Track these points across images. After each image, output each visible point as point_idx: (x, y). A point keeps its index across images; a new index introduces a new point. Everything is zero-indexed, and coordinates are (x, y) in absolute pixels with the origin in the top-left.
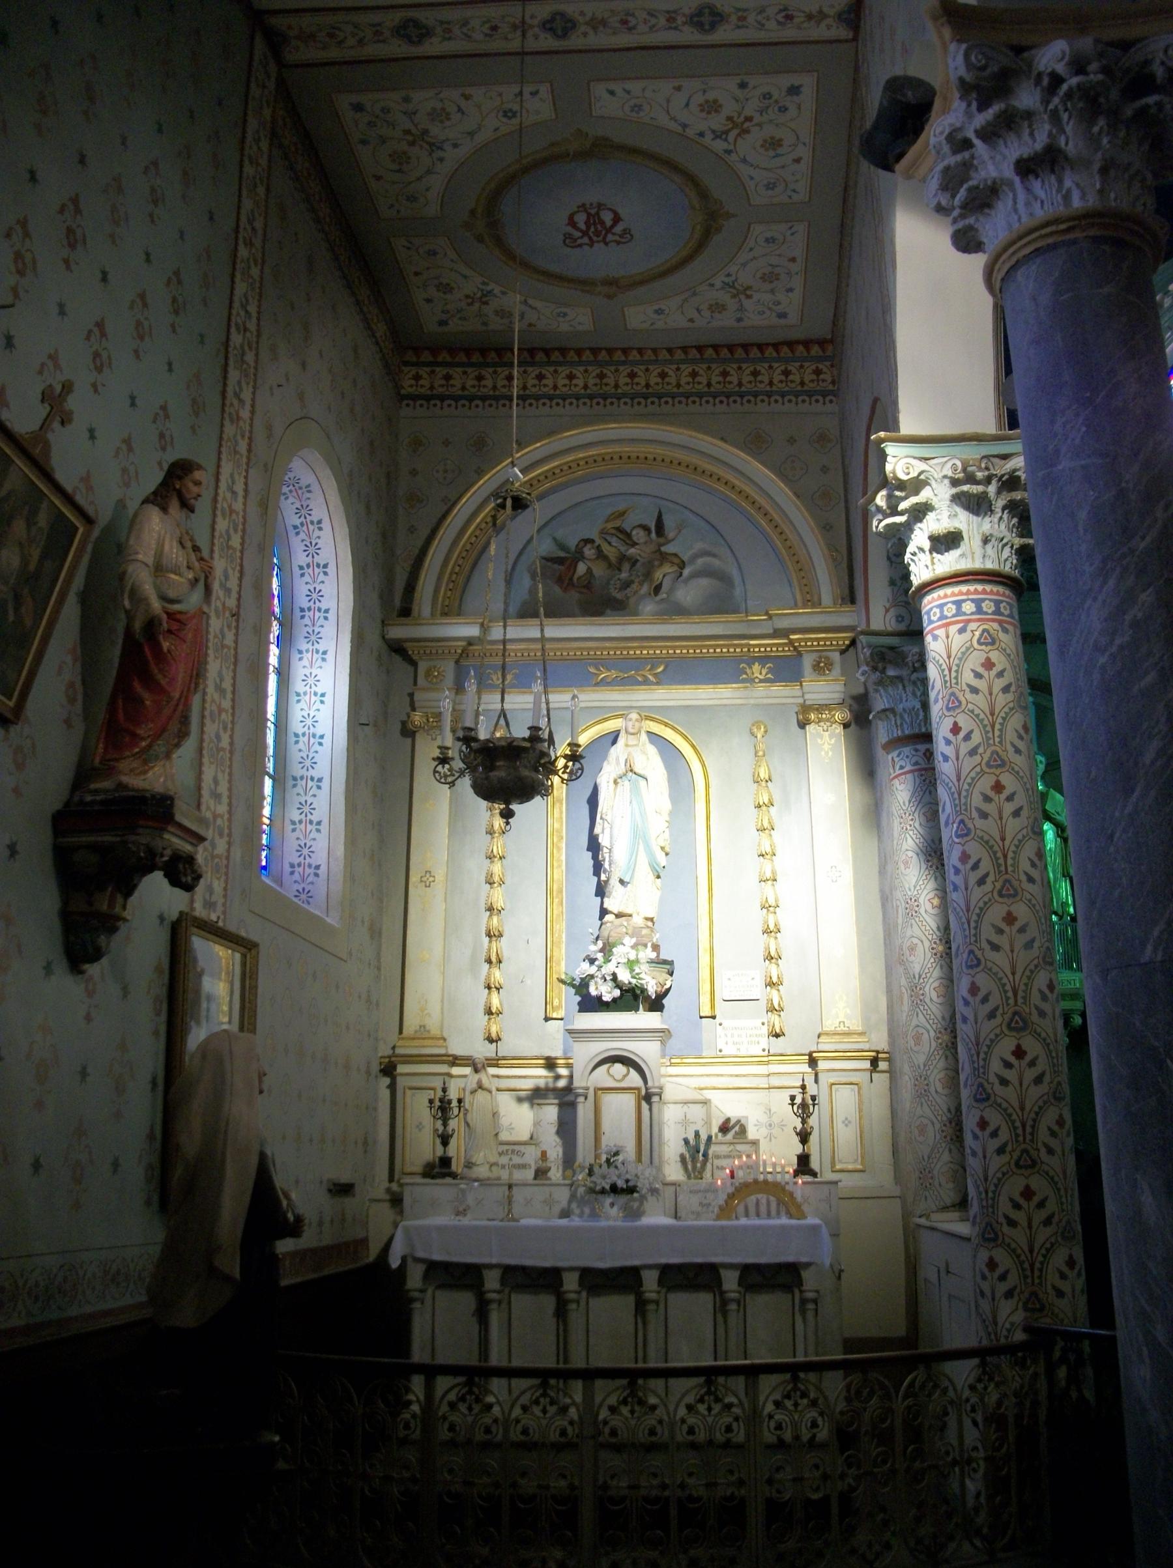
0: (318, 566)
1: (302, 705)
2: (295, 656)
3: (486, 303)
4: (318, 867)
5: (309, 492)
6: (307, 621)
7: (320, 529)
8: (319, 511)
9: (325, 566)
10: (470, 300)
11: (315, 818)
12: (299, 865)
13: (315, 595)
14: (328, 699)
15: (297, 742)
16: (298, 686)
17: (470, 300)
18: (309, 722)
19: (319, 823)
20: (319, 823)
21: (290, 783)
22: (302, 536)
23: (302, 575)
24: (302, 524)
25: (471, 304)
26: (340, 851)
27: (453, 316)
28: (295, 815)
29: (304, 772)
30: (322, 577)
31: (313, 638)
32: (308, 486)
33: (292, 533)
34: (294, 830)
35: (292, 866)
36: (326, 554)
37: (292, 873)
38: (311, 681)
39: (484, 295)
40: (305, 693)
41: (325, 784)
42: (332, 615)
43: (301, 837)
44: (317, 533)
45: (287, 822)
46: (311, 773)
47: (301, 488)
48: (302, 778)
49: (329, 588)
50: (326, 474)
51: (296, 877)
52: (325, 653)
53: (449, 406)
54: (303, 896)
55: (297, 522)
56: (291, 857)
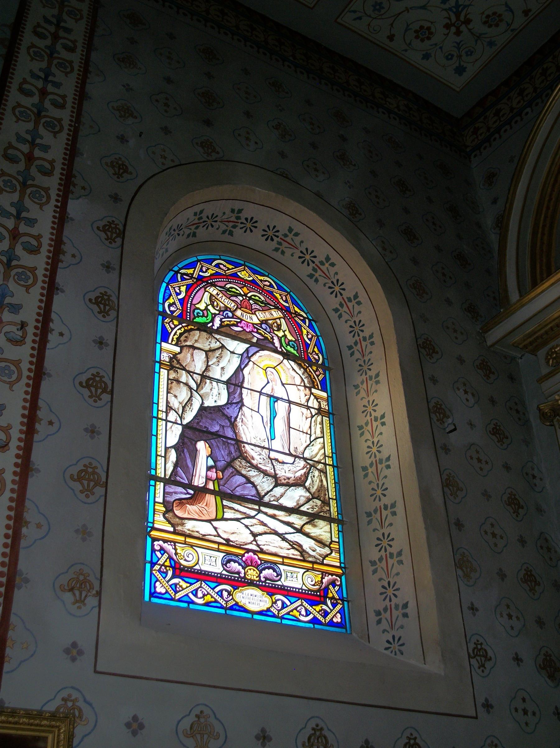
0: (350, 300)
1: (367, 436)
2: (352, 392)
3: (468, 21)
4: (405, 606)
5: (297, 235)
6: (357, 355)
7: (333, 265)
8: (322, 251)
9: (356, 296)
10: (453, 29)
11: (394, 550)
12: (385, 610)
13: (356, 328)
14: (388, 419)
15: (366, 475)
16: (359, 419)
17: (453, 29)
18: (374, 449)
19: (400, 554)
20: (400, 554)
21: (364, 519)
22: (322, 280)
23: (340, 316)
24: (314, 270)
25: (458, 33)
26: (427, 575)
27: (460, 56)
28: (373, 554)
29: (377, 504)
30: (357, 308)
31: (365, 368)
32: (290, 230)
33: (311, 283)
34: (375, 572)
35: (378, 613)
36: (352, 285)
37: (379, 622)
38: (370, 409)
39: (458, 15)
40: (367, 424)
41: (400, 509)
42: (377, 339)
43: (384, 577)
44: (332, 270)
45: (366, 564)
46: (385, 500)
47: (286, 235)
48: (375, 511)
49: (366, 315)
50: (293, 207)
51: (385, 625)
52: (377, 375)
53: (505, 131)
54: (395, 646)
55: (310, 270)
56: (375, 602)
